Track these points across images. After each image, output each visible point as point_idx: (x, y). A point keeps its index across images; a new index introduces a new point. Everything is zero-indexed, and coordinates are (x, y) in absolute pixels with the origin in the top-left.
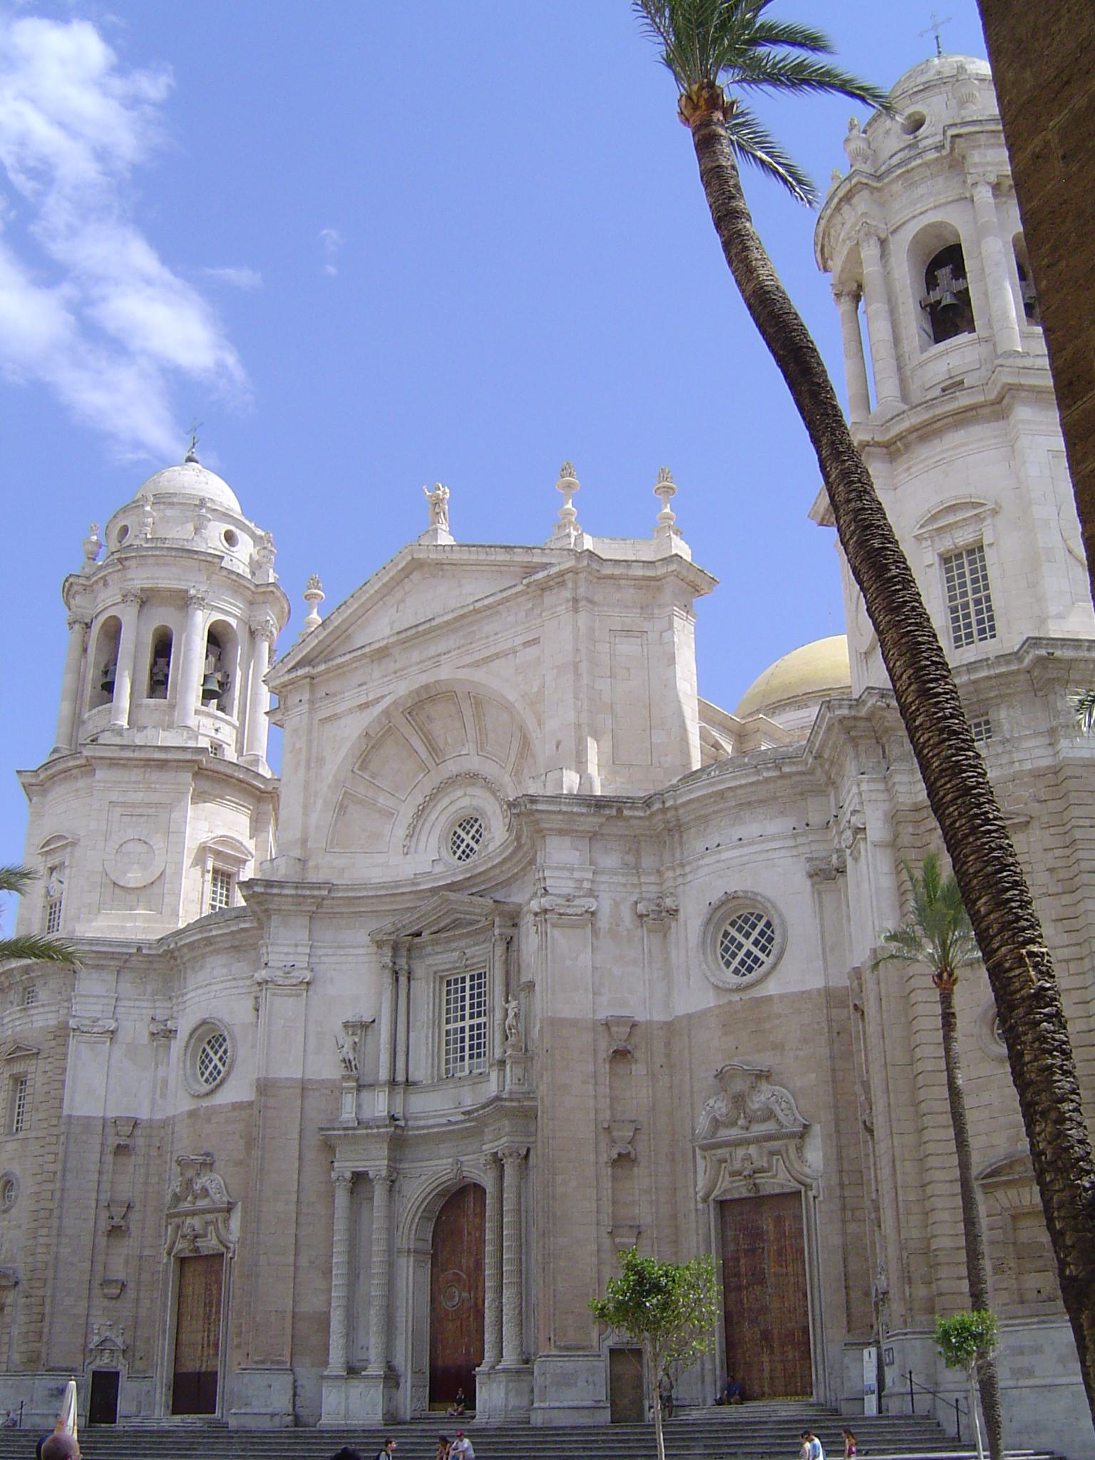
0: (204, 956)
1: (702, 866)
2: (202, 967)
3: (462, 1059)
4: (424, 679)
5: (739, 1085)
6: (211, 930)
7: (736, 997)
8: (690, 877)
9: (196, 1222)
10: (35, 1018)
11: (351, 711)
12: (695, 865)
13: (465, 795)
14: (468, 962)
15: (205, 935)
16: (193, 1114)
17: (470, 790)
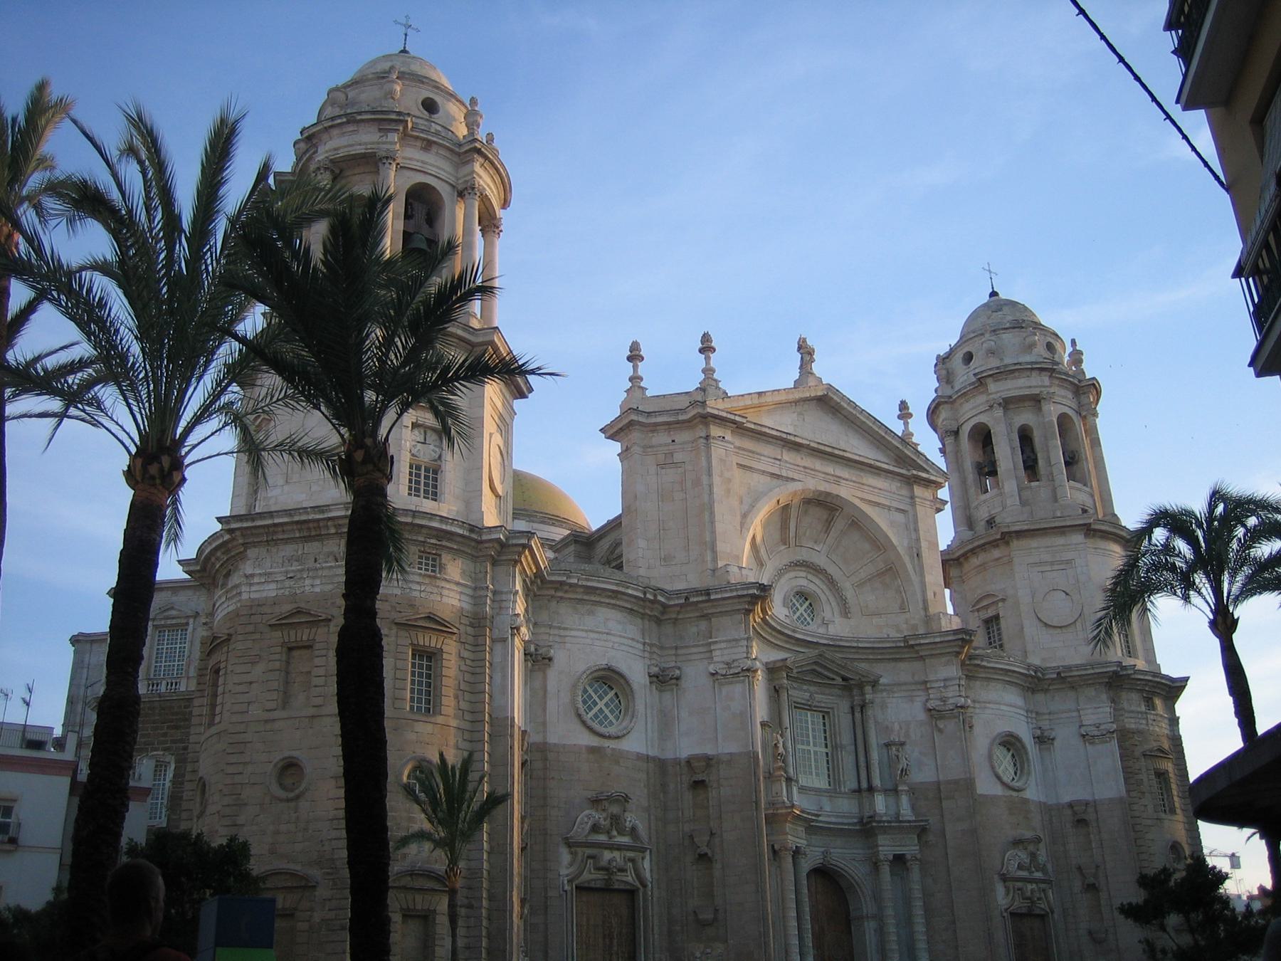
0: (599, 603)
1: (989, 708)
2: (591, 613)
3: (811, 773)
4: (824, 487)
5: (1031, 848)
6: (628, 588)
7: (1014, 794)
8: (977, 711)
9: (616, 854)
10: (445, 592)
11: (764, 472)
12: (983, 705)
13: (807, 578)
14: (817, 704)
15: (621, 589)
16: (592, 750)
17: (810, 577)
